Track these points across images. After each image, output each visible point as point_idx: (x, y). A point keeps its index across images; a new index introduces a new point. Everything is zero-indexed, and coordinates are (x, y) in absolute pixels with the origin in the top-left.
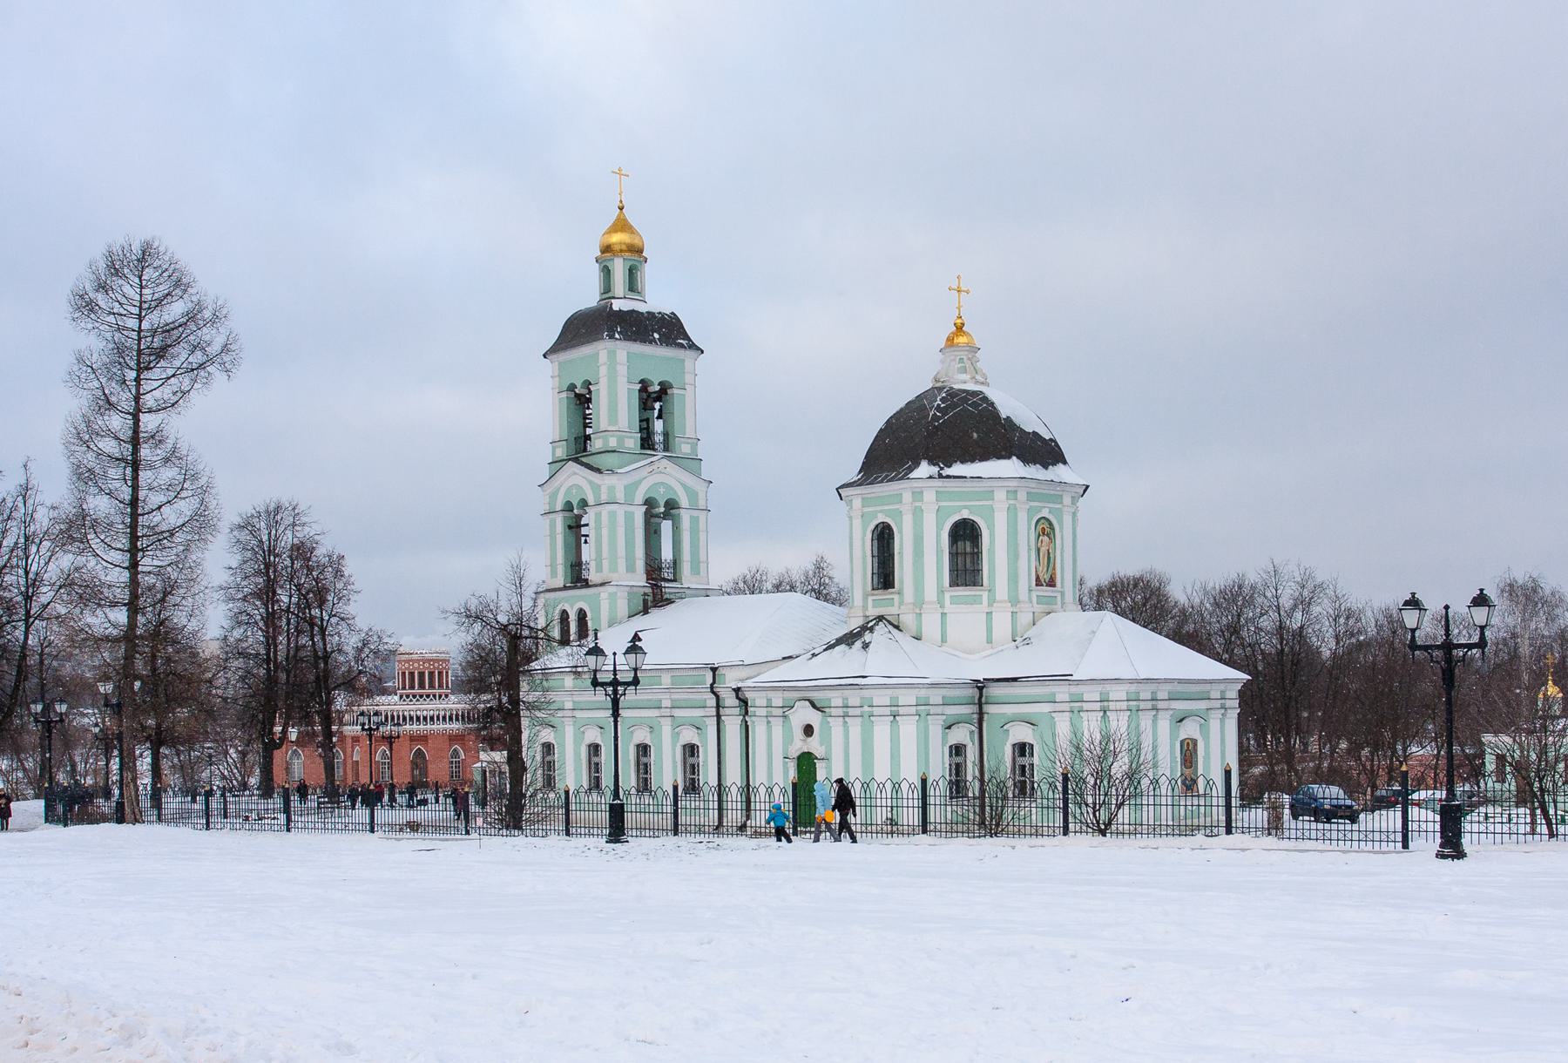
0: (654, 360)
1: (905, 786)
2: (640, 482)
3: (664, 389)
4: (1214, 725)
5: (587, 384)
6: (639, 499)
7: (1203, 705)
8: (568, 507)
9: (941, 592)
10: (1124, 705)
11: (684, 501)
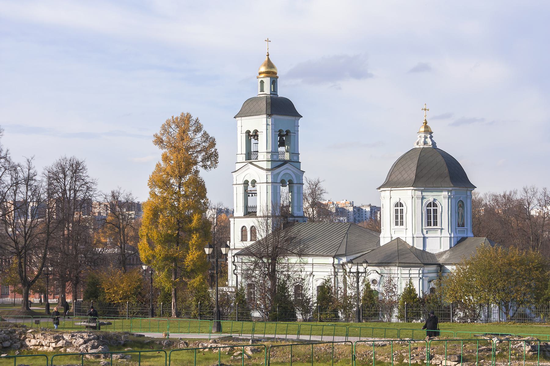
0: (285, 121)
3: (288, 132)
5: (256, 131)
6: (279, 181)
8: (246, 183)
11: (295, 182)
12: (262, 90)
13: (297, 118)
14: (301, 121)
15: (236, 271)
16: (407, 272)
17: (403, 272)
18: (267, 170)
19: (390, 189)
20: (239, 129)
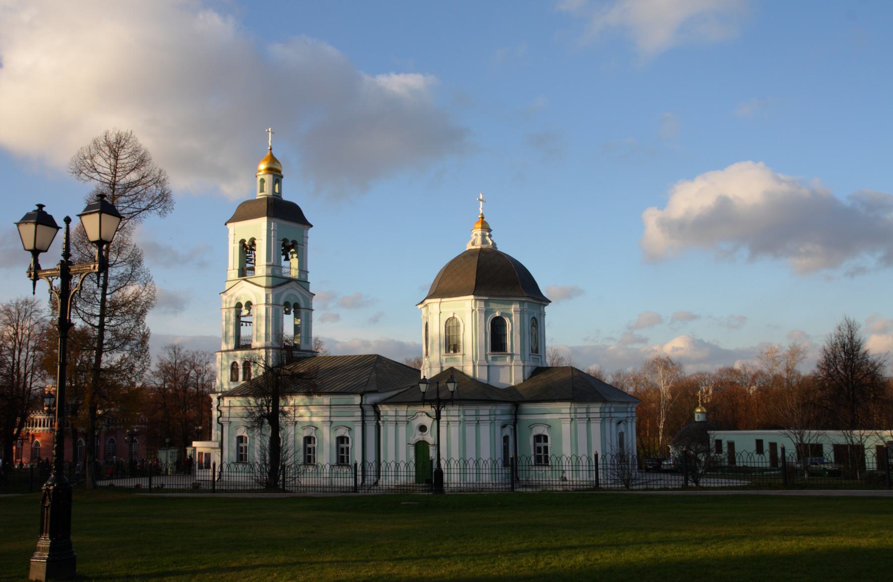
1: (564, 459)
2: (281, 294)
4: (629, 424)
5: (253, 241)
6: (282, 303)
7: (624, 415)
8: (239, 306)
9: (486, 356)
10: (598, 415)
11: (302, 305)
12: (262, 191)
13: (306, 227)
14: (311, 232)
15: (221, 419)
16: (473, 413)
17: (467, 413)
18: (266, 287)
19: (439, 300)
20: (231, 238)
